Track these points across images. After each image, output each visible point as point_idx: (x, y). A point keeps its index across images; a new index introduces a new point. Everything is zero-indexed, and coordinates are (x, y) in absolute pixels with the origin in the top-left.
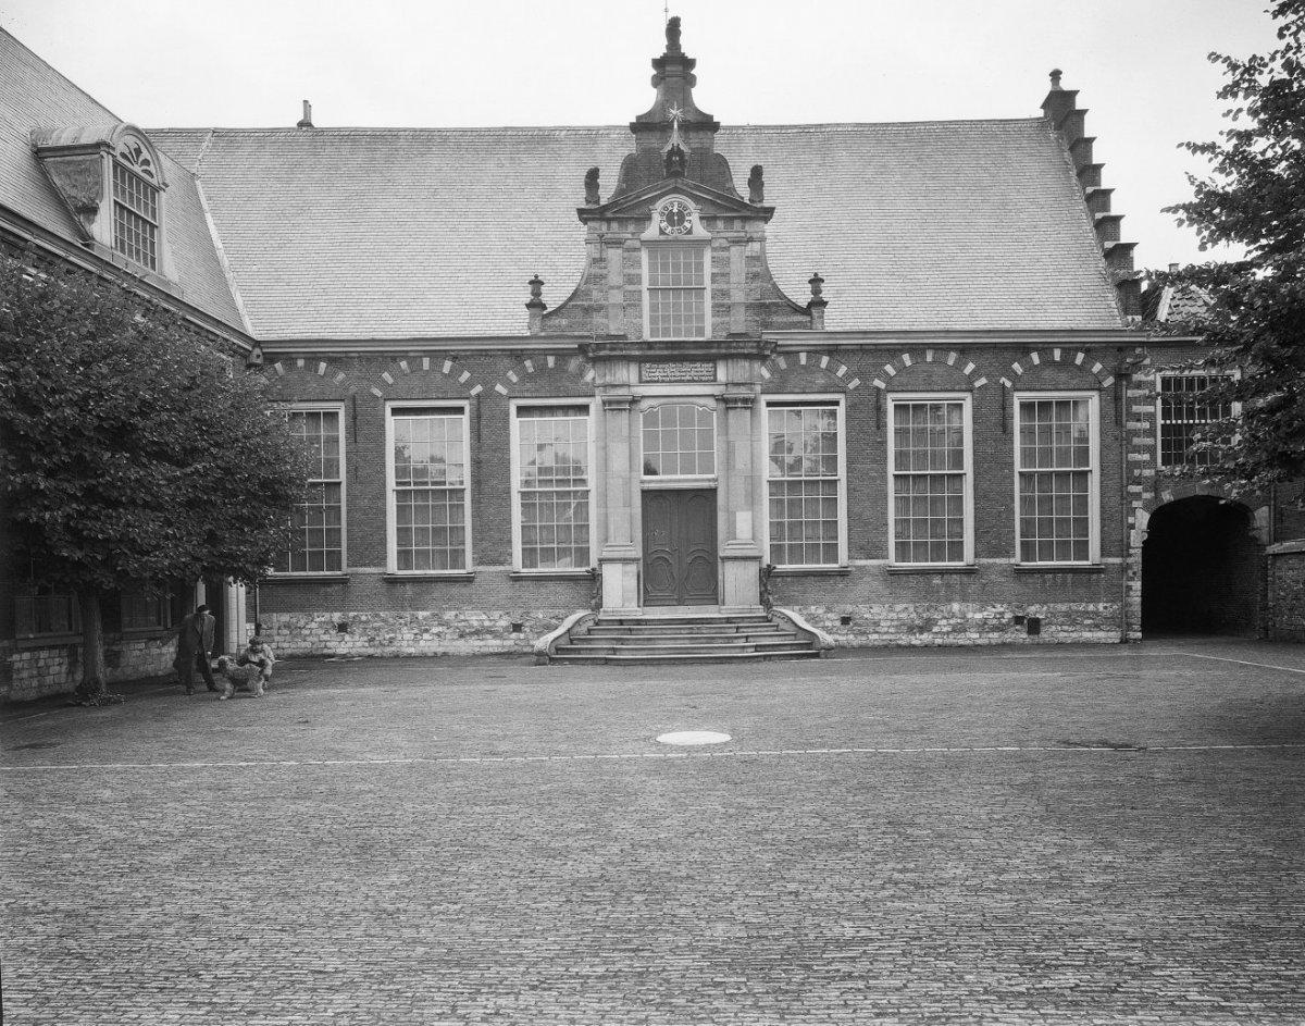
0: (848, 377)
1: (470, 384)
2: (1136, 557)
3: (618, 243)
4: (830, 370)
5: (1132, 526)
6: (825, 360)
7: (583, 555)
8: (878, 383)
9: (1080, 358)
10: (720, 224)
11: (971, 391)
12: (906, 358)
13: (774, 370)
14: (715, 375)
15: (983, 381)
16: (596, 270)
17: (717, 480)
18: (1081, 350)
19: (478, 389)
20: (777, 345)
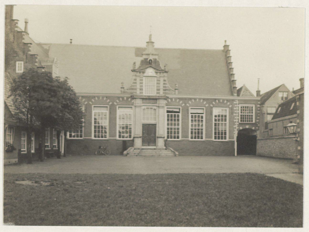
0: (182, 104)
1: (109, 102)
2: (235, 139)
3: (139, 76)
5: (234, 134)
6: (178, 100)
7: (130, 136)
8: (188, 105)
9: (105, 99)
10: (159, 73)
12: (193, 100)
13: (168, 101)
14: (157, 102)
15: (207, 105)
16: (135, 81)
17: (156, 122)
19: (111, 103)
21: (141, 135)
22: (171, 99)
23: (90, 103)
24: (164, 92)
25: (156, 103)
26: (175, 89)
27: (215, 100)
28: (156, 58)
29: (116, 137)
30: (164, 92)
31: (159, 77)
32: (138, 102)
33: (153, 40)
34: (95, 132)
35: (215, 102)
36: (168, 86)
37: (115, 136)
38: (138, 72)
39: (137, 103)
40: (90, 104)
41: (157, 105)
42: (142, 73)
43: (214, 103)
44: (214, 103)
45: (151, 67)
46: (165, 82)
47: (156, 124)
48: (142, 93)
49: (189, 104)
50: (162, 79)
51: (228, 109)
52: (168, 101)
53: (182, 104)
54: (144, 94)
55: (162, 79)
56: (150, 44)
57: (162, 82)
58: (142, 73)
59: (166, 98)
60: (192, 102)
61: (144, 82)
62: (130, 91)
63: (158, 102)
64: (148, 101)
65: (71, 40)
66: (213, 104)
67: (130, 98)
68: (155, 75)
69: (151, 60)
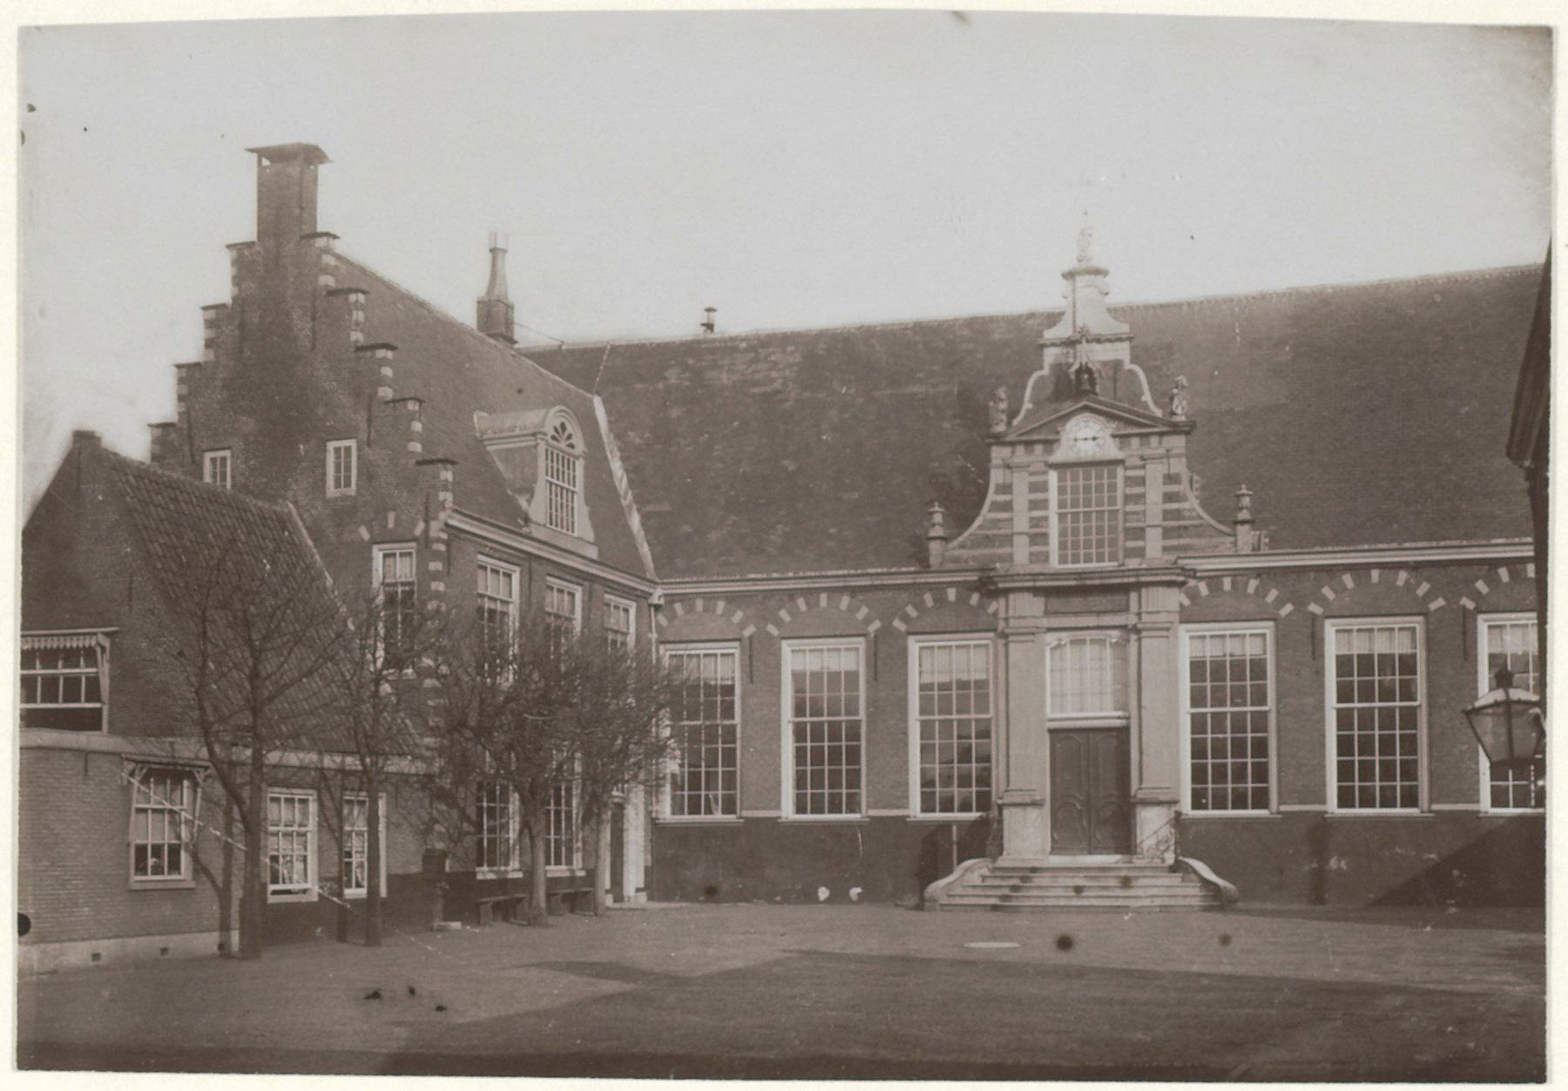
0: (1280, 603)
1: (868, 621)
4: (1261, 593)
6: (1253, 584)
7: (984, 802)
8: (1315, 608)
10: (1135, 442)
11: (739, 640)
12: (1348, 580)
13: (1194, 595)
15: (1440, 602)
16: (1002, 498)
17: (1128, 718)
18: (1227, 576)
19: (877, 625)
20: (1195, 571)
21: (1046, 792)
22: (1214, 580)
23: (772, 629)
24: (1174, 542)
25: (1126, 609)
26: (1236, 523)
27: (1494, 564)
28: (1120, 358)
29: (906, 806)
30: (1174, 542)
31: (1140, 463)
32: (1027, 607)
33: (1097, 262)
34: (1344, 771)
35: (1492, 581)
36: (1192, 510)
37: (903, 801)
38: (1020, 443)
39: (1015, 618)
40: (769, 635)
41: (1131, 620)
43: (1481, 586)
44: (1481, 586)
45: (1086, 409)
46: (1175, 488)
47: (1124, 732)
48: (1045, 558)
49: (1323, 601)
50: (1155, 472)
51: (1267, 628)
52: (1194, 595)
53: (1280, 603)
54: (1054, 564)
55: (1155, 472)
56: (1081, 281)
57: (1154, 493)
58: (1039, 449)
59: (1181, 579)
60: (1340, 590)
61: (1053, 495)
62: (977, 552)
63: (1134, 607)
64: (1076, 602)
65: (710, 310)
66: (1476, 596)
67: (977, 589)
68: (1112, 450)
69: (1089, 371)
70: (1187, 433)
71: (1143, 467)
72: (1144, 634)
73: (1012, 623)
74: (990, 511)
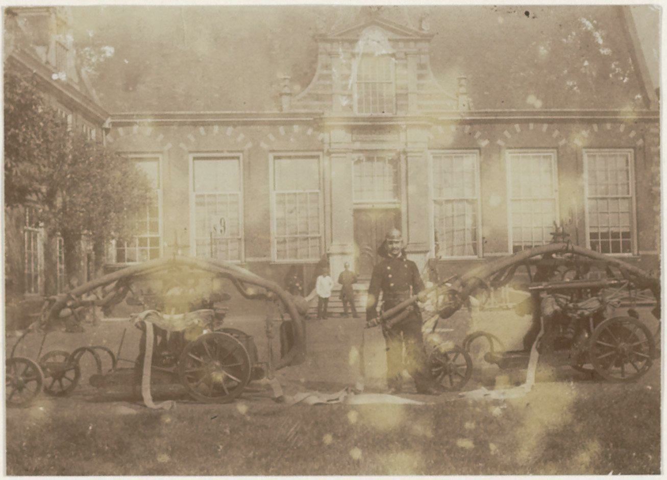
10: (401, 44)
16: (325, 72)
19: (249, 145)
23: (182, 145)
42: (347, 45)
49: (505, 138)
59: (430, 124)
70: (429, 41)
71: (406, 59)
72: (409, 154)
73: (333, 146)
74: (318, 80)
